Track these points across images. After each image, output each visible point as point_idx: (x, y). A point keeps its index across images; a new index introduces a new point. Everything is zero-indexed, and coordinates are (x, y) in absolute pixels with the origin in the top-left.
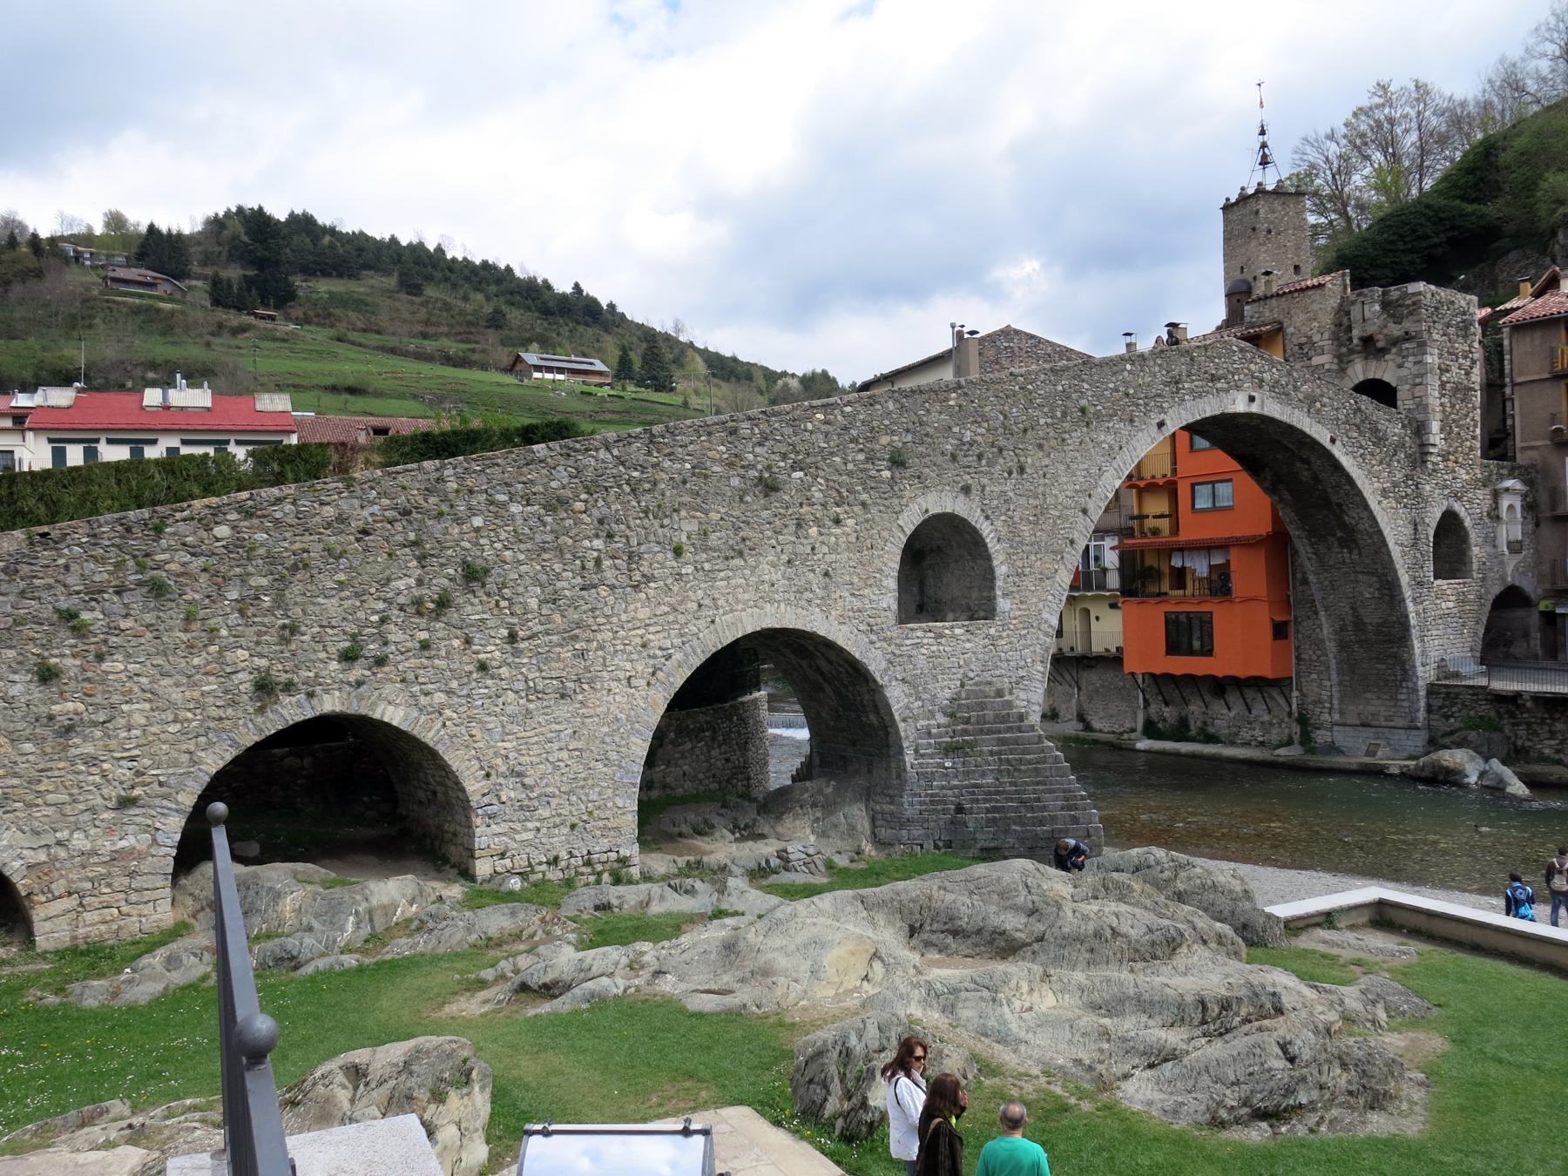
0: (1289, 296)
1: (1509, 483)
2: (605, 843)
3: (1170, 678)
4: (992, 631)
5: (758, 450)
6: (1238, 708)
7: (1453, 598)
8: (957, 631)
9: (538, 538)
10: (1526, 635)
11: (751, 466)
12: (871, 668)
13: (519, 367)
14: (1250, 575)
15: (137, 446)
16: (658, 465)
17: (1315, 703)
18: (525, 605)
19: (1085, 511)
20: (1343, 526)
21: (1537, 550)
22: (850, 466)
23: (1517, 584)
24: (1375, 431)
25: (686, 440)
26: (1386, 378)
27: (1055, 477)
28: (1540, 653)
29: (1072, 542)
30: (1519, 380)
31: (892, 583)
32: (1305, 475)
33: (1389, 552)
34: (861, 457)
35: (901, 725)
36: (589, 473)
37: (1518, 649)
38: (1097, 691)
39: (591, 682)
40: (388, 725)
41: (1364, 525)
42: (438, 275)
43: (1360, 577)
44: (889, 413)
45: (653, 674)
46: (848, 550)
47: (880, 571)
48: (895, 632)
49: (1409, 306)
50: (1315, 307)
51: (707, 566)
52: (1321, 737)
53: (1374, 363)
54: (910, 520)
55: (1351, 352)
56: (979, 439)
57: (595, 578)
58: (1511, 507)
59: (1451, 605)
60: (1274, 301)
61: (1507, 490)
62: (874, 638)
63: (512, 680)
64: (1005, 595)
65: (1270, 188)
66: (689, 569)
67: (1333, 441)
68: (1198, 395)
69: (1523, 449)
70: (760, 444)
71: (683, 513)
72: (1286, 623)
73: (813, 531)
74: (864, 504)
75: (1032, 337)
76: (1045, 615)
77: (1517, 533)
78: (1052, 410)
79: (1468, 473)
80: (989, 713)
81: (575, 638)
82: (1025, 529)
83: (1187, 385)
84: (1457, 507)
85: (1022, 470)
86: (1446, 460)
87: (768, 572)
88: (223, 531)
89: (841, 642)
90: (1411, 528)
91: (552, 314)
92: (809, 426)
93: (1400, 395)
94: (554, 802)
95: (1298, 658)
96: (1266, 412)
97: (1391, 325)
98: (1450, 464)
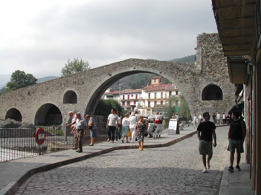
7: (212, 105)
8: (71, 105)
24: (178, 69)
31: (62, 99)
34: (59, 84)
35: (62, 115)
59: (211, 106)
67: (161, 73)
68: (120, 69)
76: (85, 103)
78: (89, 76)
79: (222, 75)
81: (31, 103)
83: (118, 68)
84: (215, 83)
87: (49, 98)
88: (9, 94)
90: (192, 89)
96: (139, 70)
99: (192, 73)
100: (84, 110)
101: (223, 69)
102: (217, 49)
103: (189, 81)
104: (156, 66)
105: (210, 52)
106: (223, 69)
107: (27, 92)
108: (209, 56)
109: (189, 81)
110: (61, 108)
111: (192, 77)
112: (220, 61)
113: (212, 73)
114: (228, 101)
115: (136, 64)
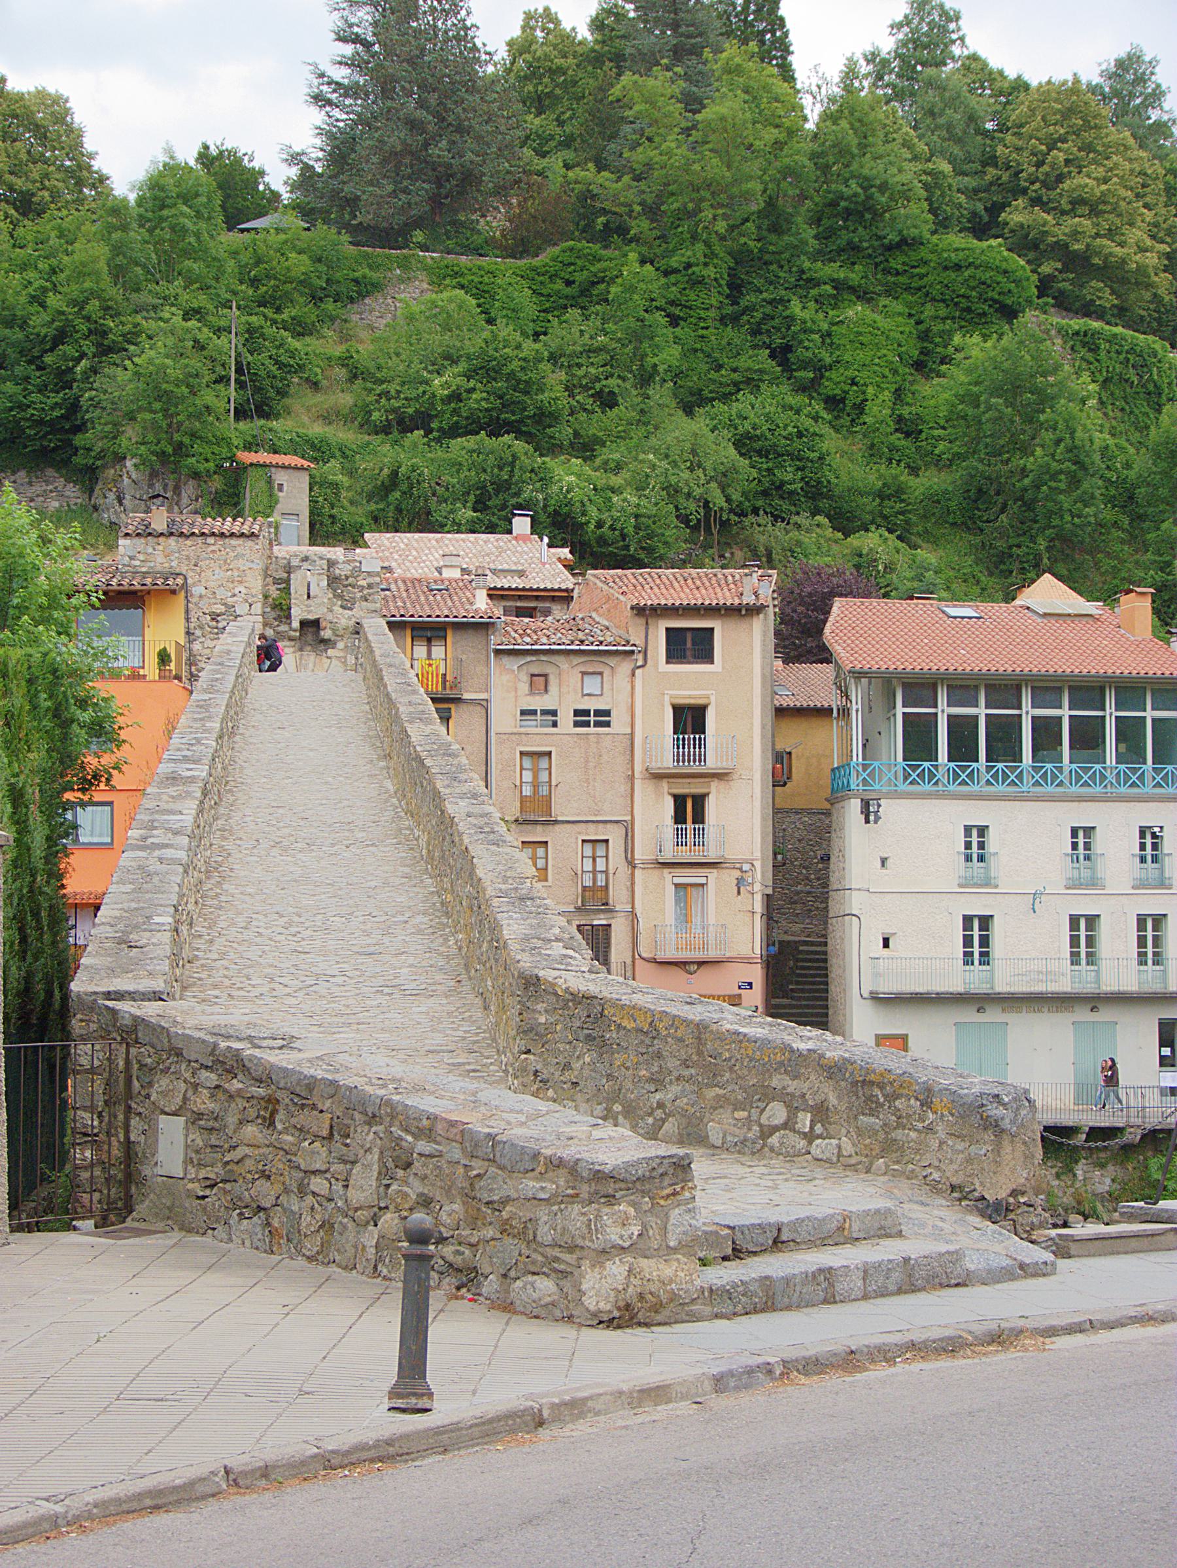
0: (200, 540)
49: (363, 587)
50: (241, 564)
53: (313, 656)
60: (172, 541)
97: (337, 609)
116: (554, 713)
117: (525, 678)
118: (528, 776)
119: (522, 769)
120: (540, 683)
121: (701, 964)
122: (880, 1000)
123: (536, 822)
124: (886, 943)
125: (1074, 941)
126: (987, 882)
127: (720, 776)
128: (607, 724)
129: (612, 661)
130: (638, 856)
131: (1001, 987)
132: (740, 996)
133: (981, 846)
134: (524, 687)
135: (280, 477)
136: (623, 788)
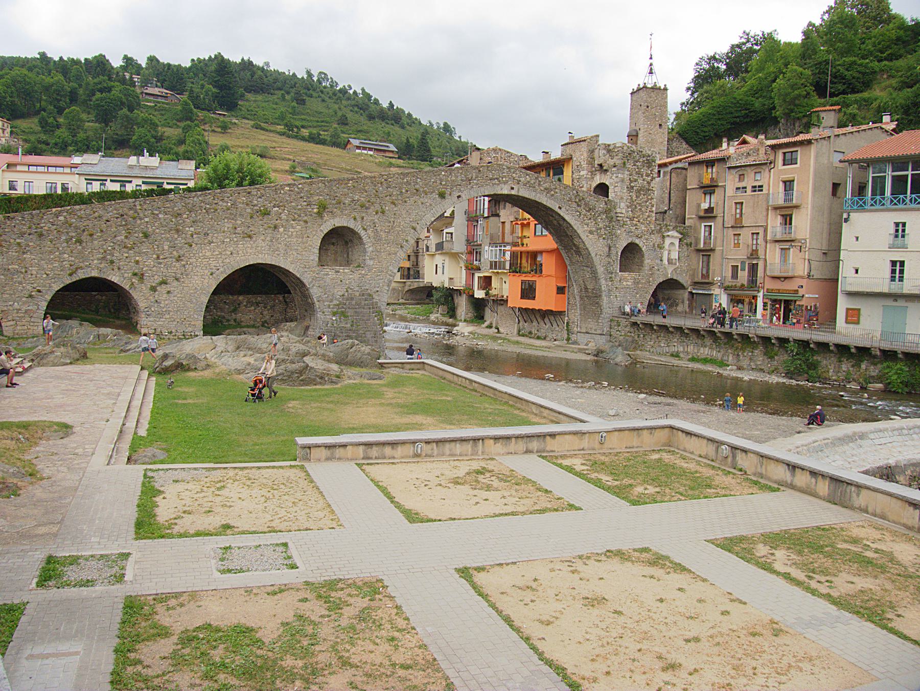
1: (669, 233)
2: (190, 329)
3: (526, 309)
4: (363, 272)
5: (259, 199)
6: (549, 325)
8: (346, 271)
9: (169, 226)
10: (683, 302)
11: (254, 206)
12: (305, 281)
13: (349, 146)
14: (548, 264)
15: (123, 183)
16: (216, 204)
17: (573, 322)
18: (163, 247)
19: (414, 229)
20: (575, 245)
21: (689, 264)
22: (300, 207)
23: (675, 278)
25: (229, 195)
26: (607, 183)
27: (400, 215)
28: (687, 310)
29: (407, 241)
30: (689, 187)
32: (555, 222)
33: (592, 258)
34: (305, 203)
35: (317, 303)
36: (190, 206)
37: (680, 308)
38: (503, 315)
39: (187, 275)
40: (113, 282)
41: (581, 246)
42: (315, 94)
43: (585, 268)
44: (319, 188)
45: (211, 274)
46: (296, 237)
47: (311, 246)
48: (318, 268)
50: (583, 149)
51: (235, 239)
52: (573, 337)
54: (327, 227)
55: (596, 171)
56: (362, 199)
57: (190, 241)
58: (672, 244)
59: (629, 283)
60: (570, 146)
61: (668, 236)
62: (306, 270)
63: (157, 272)
64: (370, 259)
65: (649, 86)
66: (228, 240)
67: (560, 208)
69: (688, 218)
70: (260, 198)
71: (226, 221)
72: (565, 287)
73: (281, 230)
74: (306, 222)
75: (508, 152)
76: (391, 268)
77: (674, 255)
78: (400, 188)
80: (354, 302)
81: (182, 260)
82: (383, 235)
84: (637, 241)
85: (383, 212)
86: (631, 219)
89: (291, 270)
91: (374, 118)
92: (282, 192)
93: (610, 191)
94: (171, 314)
95: (568, 303)
98: (635, 222)
99: (606, 217)
100: (388, 286)
101: (649, 216)
102: (644, 177)
103: (603, 232)
104: (553, 192)
105: (636, 180)
106: (649, 216)
107: (160, 216)
108: (632, 187)
109: (603, 232)
110: (312, 282)
111: (607, 224)
112: (646, 202)
113: (635, 222)
114: (651, 274)
115: (514, 179)
116: (745, 188)
117: (737, 176)
118: (738, 211)
119: (736, 209)
120: (741, 177)
121: (785, 278)
122: (851, 294)
123: (737, 227)
124: (857, 271)
125: (893, 271)
126: (904, 247)
127: (797, 207)
128: (762, 190)
129: (764, 167)
130: (768, 238)
131: (905, 291)
132: (797, 291)
133: (903, 231)
134: (737, 180)
135: (822, 115)
136: (765, 213)
